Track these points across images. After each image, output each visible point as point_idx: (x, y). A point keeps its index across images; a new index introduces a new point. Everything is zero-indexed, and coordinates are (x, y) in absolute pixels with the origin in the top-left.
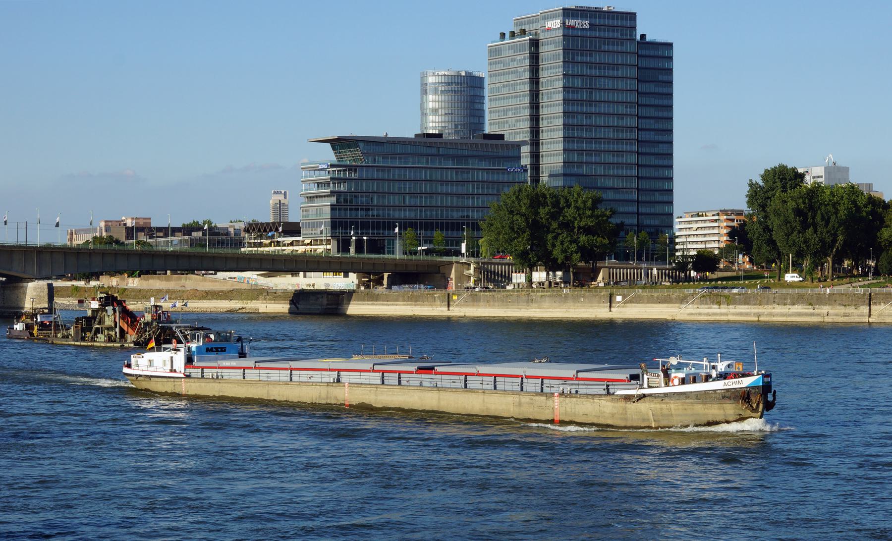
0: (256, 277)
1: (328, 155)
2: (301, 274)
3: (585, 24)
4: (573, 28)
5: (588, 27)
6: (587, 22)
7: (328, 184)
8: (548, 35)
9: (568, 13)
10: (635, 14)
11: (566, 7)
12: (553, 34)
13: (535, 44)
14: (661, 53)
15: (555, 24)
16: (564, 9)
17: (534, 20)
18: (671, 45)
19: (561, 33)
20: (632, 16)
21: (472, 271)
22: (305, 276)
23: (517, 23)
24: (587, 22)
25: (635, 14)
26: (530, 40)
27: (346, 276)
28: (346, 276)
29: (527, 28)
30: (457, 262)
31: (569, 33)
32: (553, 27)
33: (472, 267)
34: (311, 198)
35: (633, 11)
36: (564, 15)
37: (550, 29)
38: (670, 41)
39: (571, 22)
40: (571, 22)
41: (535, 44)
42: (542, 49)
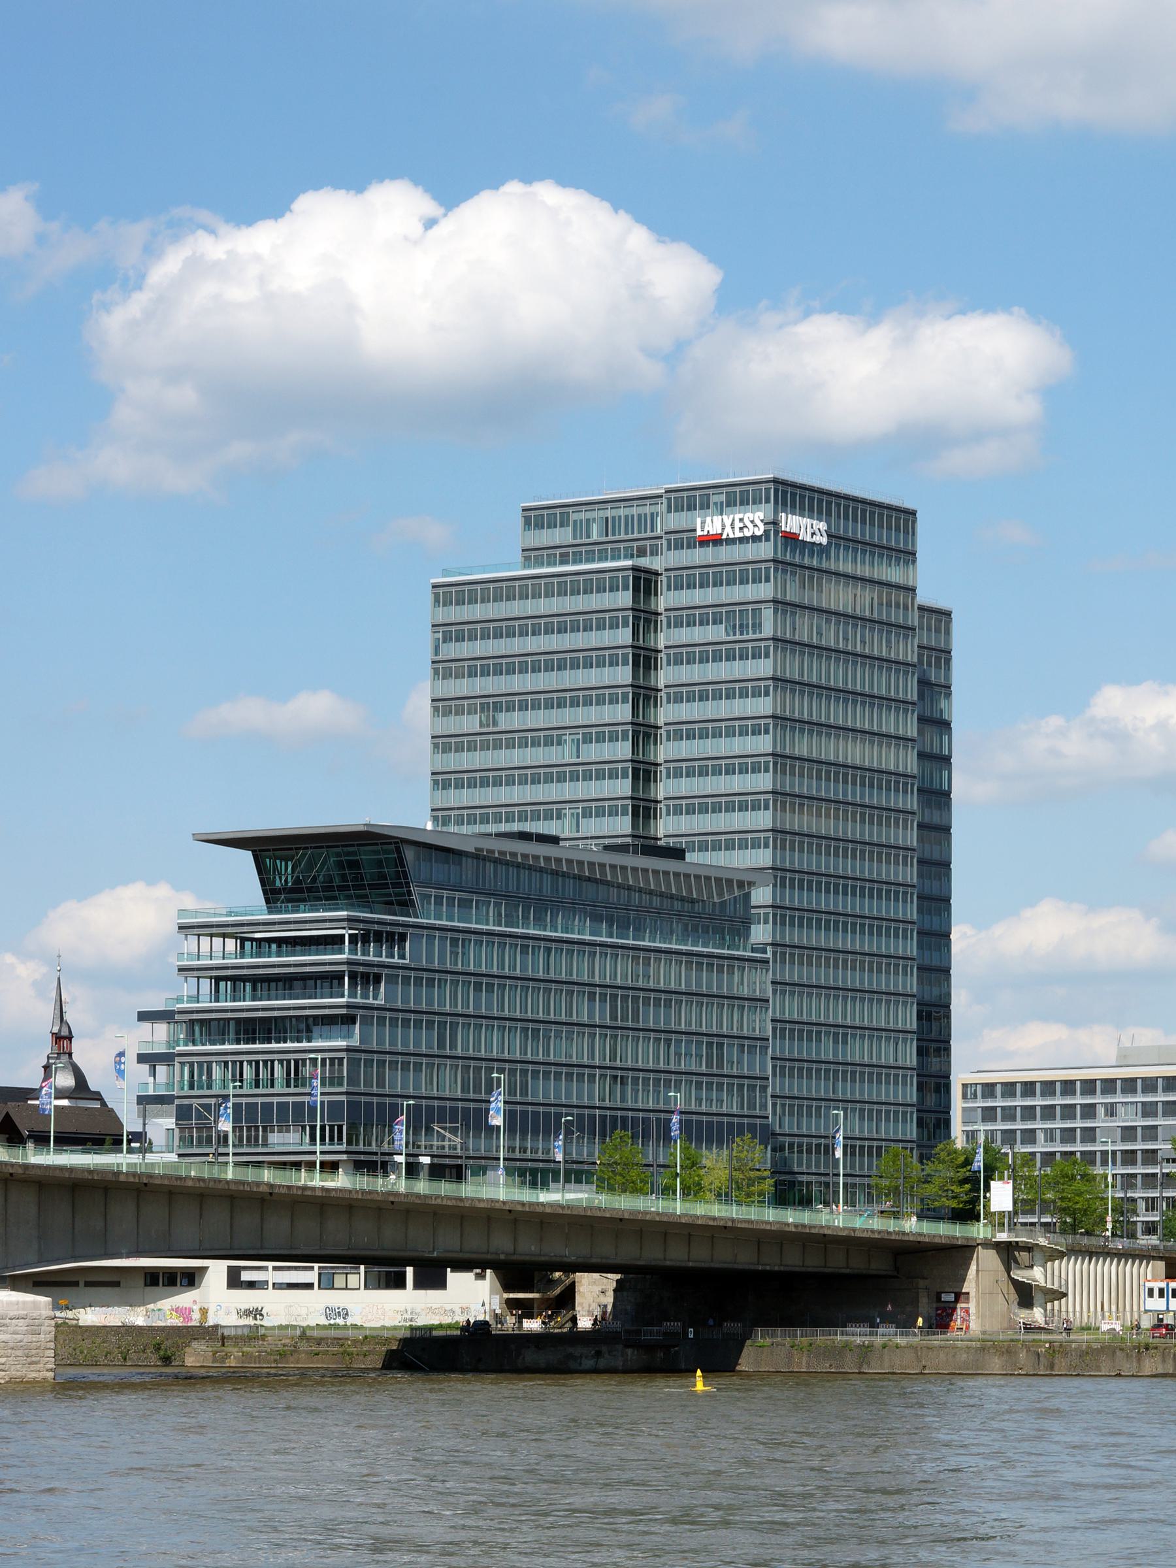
1: (238, 887)
3: (808, 528)
4: (791, 539)
7: (339, 977)
9: (789, 494)
10: (914, 513)
16: (776, 481)
22: (234, 1281)
24: (823, 526)
25: (914, 513)
30: (988, 1244)
32: (728, 533)
34: (205, 1026)
35: (908, 504)
37: (716, 540)
39: (793, 523)
40: (793, 523)
42: (664, 601)
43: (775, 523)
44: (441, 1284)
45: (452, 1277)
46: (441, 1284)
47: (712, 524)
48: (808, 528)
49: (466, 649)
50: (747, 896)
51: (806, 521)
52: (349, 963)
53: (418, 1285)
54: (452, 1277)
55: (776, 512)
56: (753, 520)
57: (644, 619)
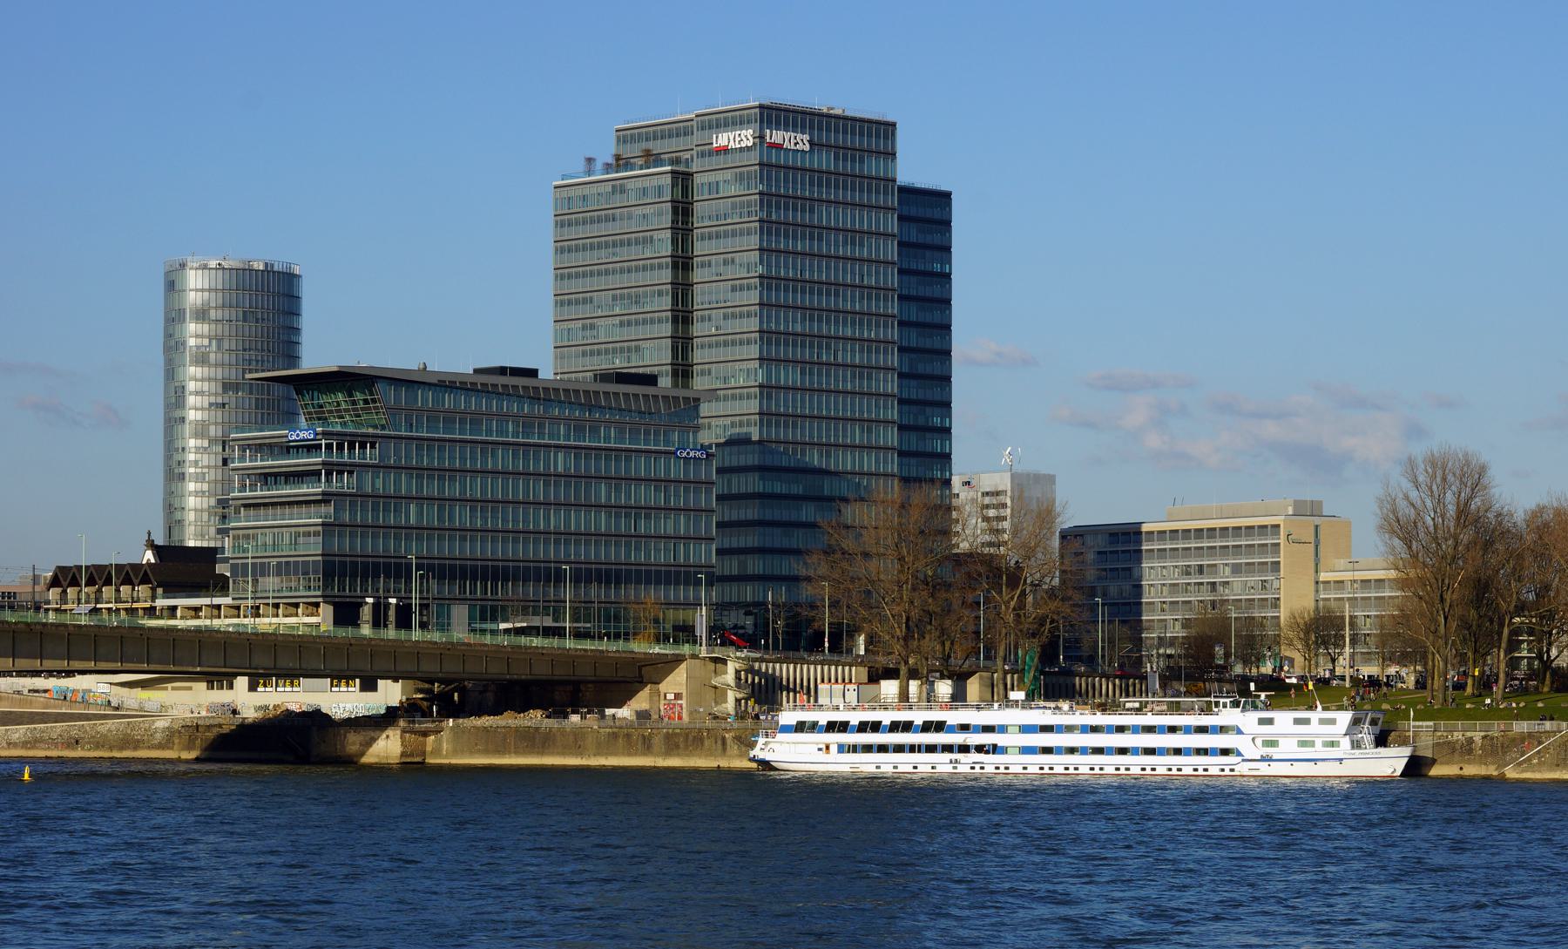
0: (105, 688)
2: (242, 682)
3: (795, 141)
4: (779, 147)
5: (807, 147)
6: (806, 137)
7: (318, 473)
8: (719, 161)
9: (772, 115)
10: (894, 125)
11: (766, 102)
12: (738, 160)
13: (683, 179)
14: (927, 214)
15: (745, 137)
16: (761, 107)
17: (680, 130)
18: (946, 196)
19: (754, 158)
20: (886, 129)
21: (730, 677)
22: (253, 687)
23: (625, 136)
25: (894, 125)
26: (672, 172)
27: (369, 685)
28: (369, 685)
29: (657, 147)
31: (772, 165)
32: (732, 145)
33: (731, 667)
35: (890, 119)
36: (762, 121)
37: (725, 150)
38: (944, 188)
39: (777, 136)
40: (777, 136)
41: (683, 179)
43: (762, 137)
44: (374, 688)
45: (380, 683)
46: (374, 688)
47: (723, 139)
48: (795, 141)
49: (580, 231)
50: (696, 408)
51: (787, 135)
52: (324, 463)
53: (364, 688)
54: (380, 683)
55: (761, 129)
56: (745, 137)
57: (682, 211)
